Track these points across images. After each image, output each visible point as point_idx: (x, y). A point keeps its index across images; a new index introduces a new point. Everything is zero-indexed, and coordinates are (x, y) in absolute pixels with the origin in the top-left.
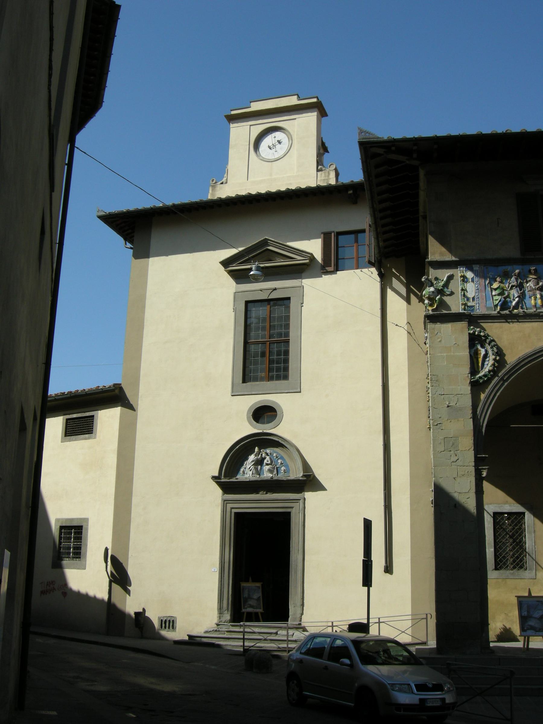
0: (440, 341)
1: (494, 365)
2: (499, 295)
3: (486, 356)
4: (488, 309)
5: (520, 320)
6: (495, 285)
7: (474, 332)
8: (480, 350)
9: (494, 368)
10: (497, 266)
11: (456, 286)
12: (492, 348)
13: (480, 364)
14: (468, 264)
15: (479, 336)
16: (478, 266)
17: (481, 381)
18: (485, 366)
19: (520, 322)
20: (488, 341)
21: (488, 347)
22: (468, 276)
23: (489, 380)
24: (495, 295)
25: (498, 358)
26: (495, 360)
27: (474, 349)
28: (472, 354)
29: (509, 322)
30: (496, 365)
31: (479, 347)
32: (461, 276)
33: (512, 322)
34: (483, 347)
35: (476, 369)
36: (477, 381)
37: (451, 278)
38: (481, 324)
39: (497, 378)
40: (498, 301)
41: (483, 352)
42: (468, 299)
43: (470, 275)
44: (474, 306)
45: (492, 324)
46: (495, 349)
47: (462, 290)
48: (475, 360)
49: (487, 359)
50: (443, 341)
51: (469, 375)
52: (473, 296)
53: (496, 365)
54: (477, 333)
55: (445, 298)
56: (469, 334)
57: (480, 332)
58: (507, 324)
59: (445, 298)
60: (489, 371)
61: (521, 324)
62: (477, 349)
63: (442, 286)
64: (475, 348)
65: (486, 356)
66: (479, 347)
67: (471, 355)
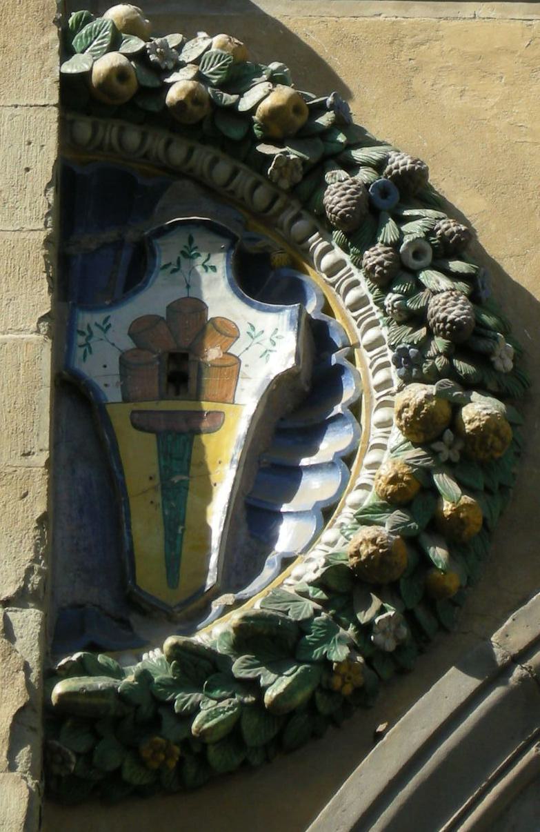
1: (412, 495)
3: (307, 400)
7: (155, 69)
8: (229, 332)
9: (413, 542)
12: (397, 274)
13: (216, 516)
15: (212, 121)
17: (209, 711)
18: (288, 535)
20: (337, 190)
21: (340, 280)
23: (335, 718)
25: (478, 409)
26: (427, 428)
27: (126, 314)
28: (101, 367)
30: (451, 496)
31: (218, 293)
34: (264, 279)
35: (150, 578)
36: (146, 711)
39: (454, 686)
41: (263, 346)
46: (443, 296)
48: (139, 455)
49: (332, 444)
51: (28, 622)
53: (451, 496)
54: (180, 85)
56: (74, 91)
57: (237, 79)
60: (344, 585)
64: (155, 298)
65: (307, 400)
66: (218, 293)
67: (71, 391)
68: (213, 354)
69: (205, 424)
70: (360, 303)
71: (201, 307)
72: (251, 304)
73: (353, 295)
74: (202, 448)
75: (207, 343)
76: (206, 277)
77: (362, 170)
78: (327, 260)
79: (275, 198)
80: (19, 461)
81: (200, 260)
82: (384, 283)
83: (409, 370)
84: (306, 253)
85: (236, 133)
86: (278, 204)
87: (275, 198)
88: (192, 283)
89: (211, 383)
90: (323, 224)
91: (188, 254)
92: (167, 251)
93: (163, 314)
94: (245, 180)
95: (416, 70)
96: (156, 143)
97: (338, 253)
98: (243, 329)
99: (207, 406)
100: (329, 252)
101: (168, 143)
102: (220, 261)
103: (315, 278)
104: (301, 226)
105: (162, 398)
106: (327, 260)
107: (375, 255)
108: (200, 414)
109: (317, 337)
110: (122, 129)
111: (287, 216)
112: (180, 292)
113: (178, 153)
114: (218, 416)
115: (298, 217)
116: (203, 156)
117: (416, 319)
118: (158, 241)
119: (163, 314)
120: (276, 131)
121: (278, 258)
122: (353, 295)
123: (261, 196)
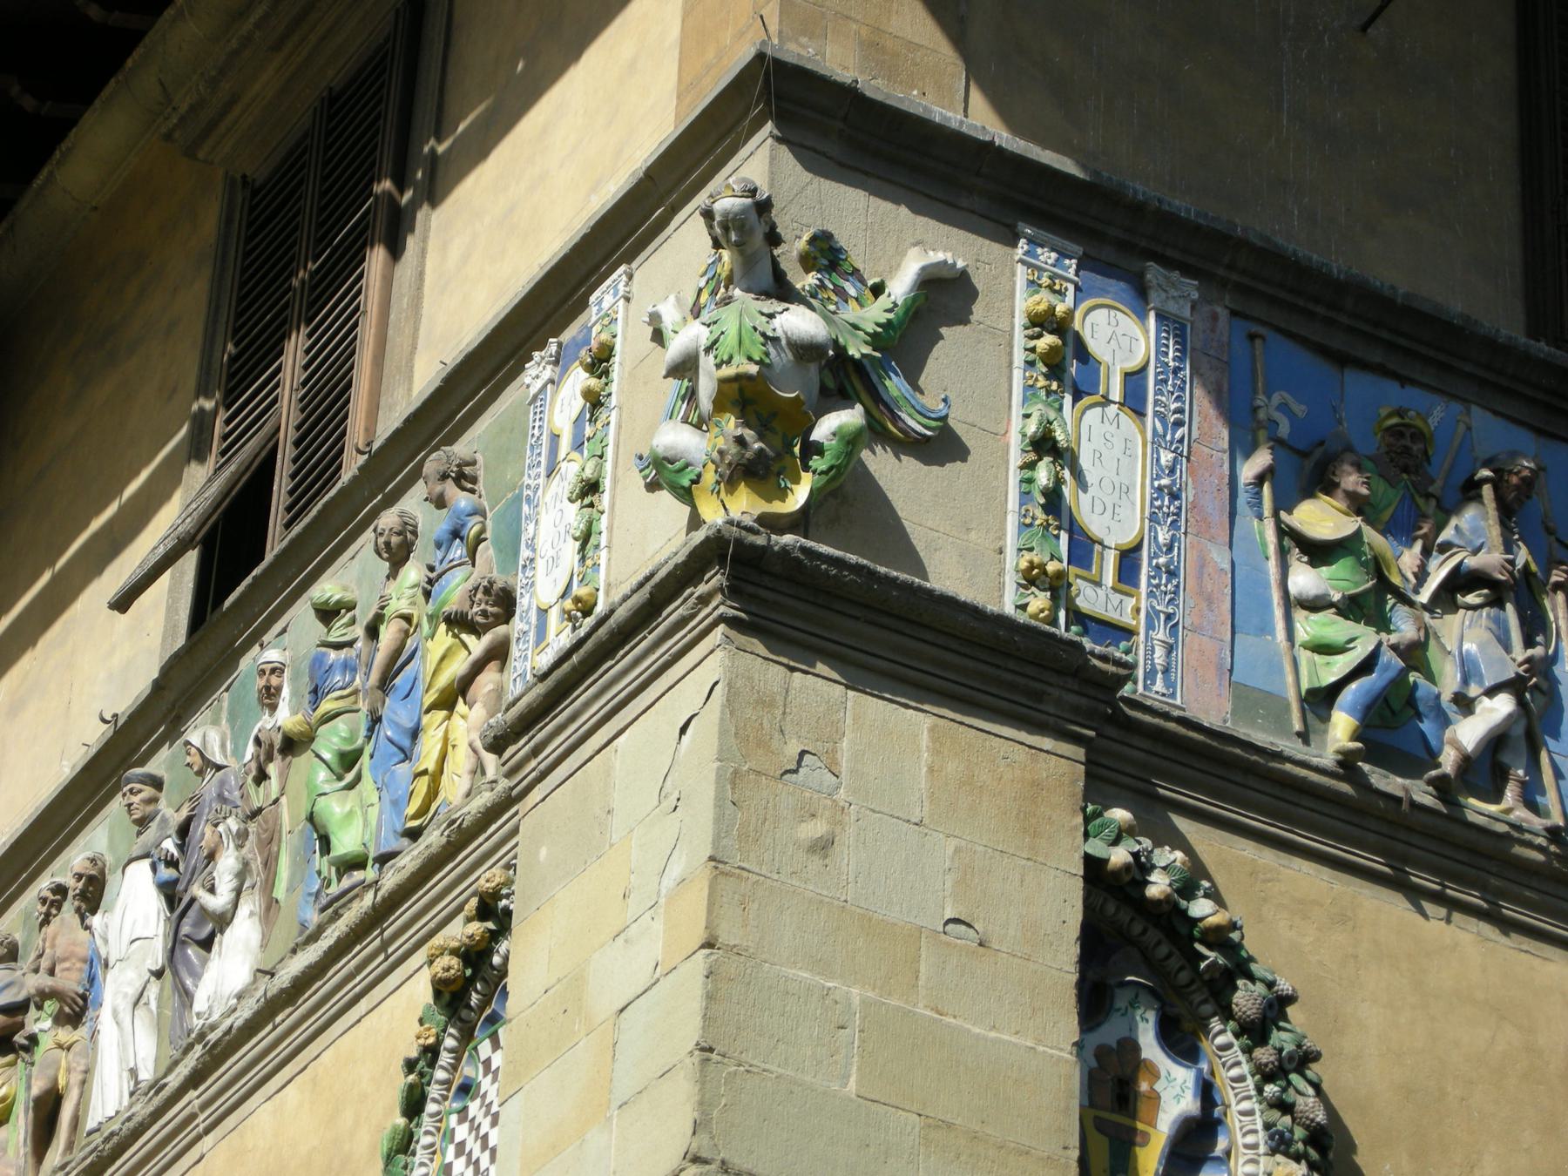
0: (823, 847)
2: (1352, 608)
4: (1246, 699)
5: (1510, 911)
6: (1321, 518)
7: (1141, 867)
10: (1342, 360)
11: (981, 378)
14: (1114, 234)
16: (1191, 288)
19: (1508, 926)
22: (1095, 346)
24: (1315, 605)
29: (1415, 895)
32: (1041, 322)
33: (1438, 898)
34: (1181, 1040)
37: (944, 296)
38: (1182, 824)
40: (1339, 666)
42: (1083, 548)
43: (1120, 336)
44: (1129, 633)
45: (1268, 857)
47: (1043, 444)
50: (847, 857)
52: (1127, 538)
55: (881, 464)
58: (1395, 906)
59: (881, 464)
61: (1517, 939)
62: (1130, 1047)
63: (875, 340)
68: (1144, 1086)
69: (1138, 1139)
70: (1241, 1079)
71: (1136, 1048)
72: (1169, 1056)
73: (1234, 1072)
74: (1135, 1157)
75: (1141, 1076)
76: (1141, 1025)
77: (1258, 984)
78: (1220, 1040)
79: (1192, 982)
80: (1061, 1152)
81: (1139, 1012)
82: (1267, 1075)
83: (1279, 1145)
84: (1206, 1029)
85: (1183, 930)
86: (1194, 987)
87: (1192, 982)
88: (1133, 1028)
89: (1143, 1108)
90: (1227, 1013)
91: (1133, 1004)
92: (1121, 1001)
93: (1114, 1045)
94: (1174, 963)
95: (1265, 900)
96: (1125, 916)
97: (1228, 1037)
98: (1163, 1073)
99: (1140, 1126)
100: (1221, 1034)
101: (1132, 920)
102: (1151, 1016)
103: (1206, 1046)
104: (1207, 1008)
105: (1113, 1111)
106: (1220, 1040)
107: (1264, 1055)
108: (1134, 1130)
109: (1206, 1091)
110: (1105, 900)
111: (1197, 998)
112: (1125, 1033)
113: (1137, 928)
114: (1146, 1136)
115: (1205, 1001)
116: (1153, 935)
117: (1285, 1107)
118: (1117, 991)
119: (1114, 1045)
120: (1211, 938)
121: (1187, 1026)
122: (1234, 1072)
123: (1184, 977)
